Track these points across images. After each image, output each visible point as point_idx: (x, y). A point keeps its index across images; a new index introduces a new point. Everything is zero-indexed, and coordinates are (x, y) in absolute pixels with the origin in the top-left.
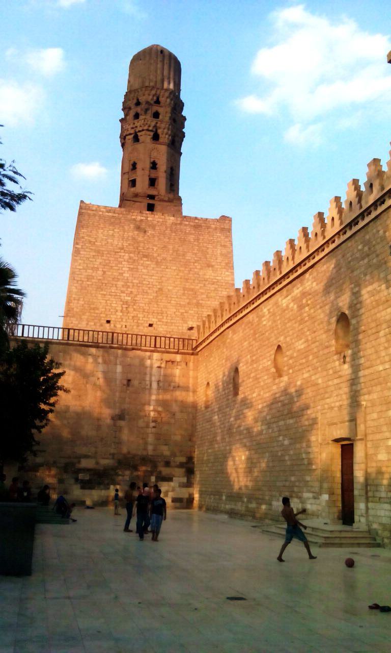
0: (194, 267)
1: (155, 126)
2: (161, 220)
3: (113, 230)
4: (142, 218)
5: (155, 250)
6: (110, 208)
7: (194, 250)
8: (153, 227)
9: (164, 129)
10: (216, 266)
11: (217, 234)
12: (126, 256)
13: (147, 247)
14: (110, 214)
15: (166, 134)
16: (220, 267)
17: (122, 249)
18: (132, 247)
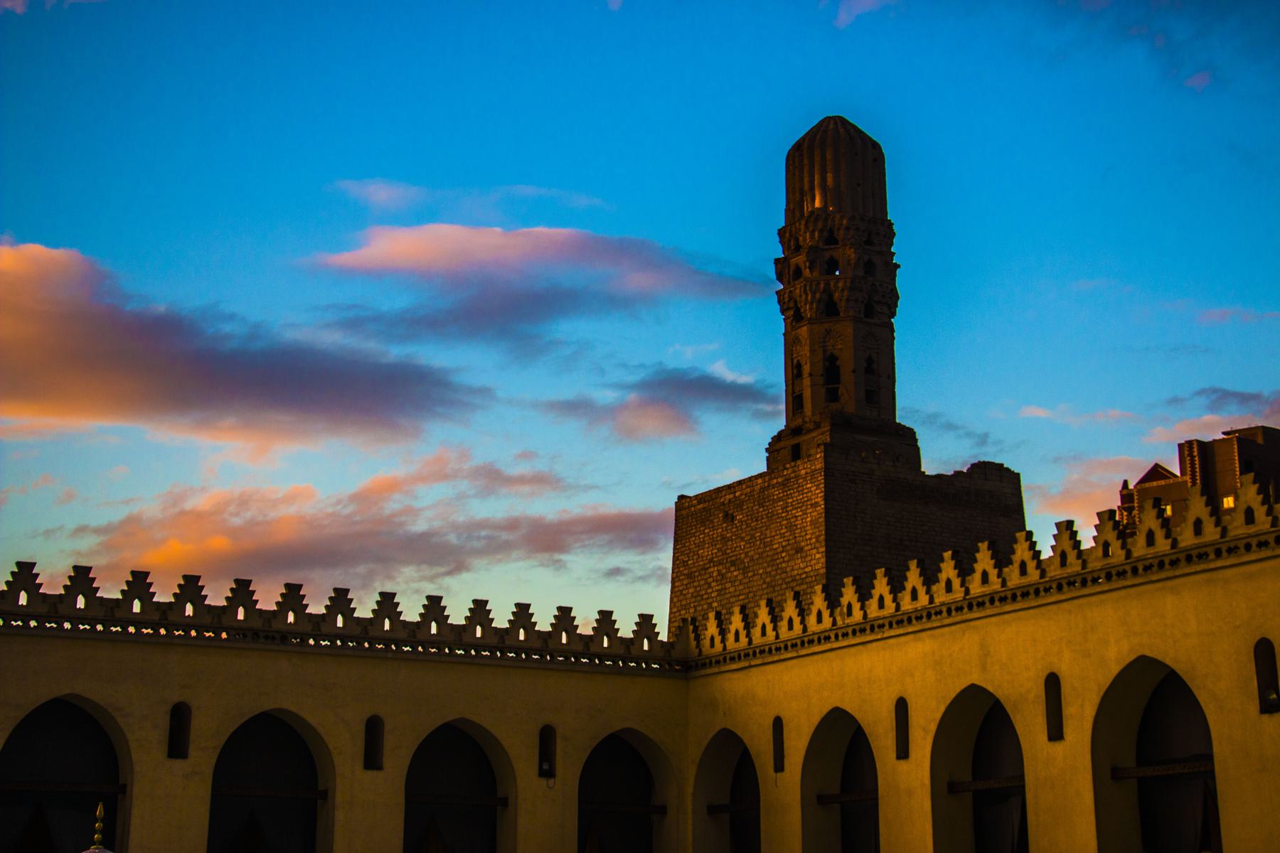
0: (781, 560)
1: (790, 298)
2: (748, 490)
3: (704, 533)
4: (731, 496)
5: (742, 547)
6: (700, 496)
7: (782, 529)
8: (740, 506)
9: (800, 296)
10: (806, 548)
11: (809, 486)
12: (715, 574)
13: (735, 545)
14: (701, 505)
15: (806, 304)
16: (810, 547)
17: (711, 561)
18: (720, 554)
